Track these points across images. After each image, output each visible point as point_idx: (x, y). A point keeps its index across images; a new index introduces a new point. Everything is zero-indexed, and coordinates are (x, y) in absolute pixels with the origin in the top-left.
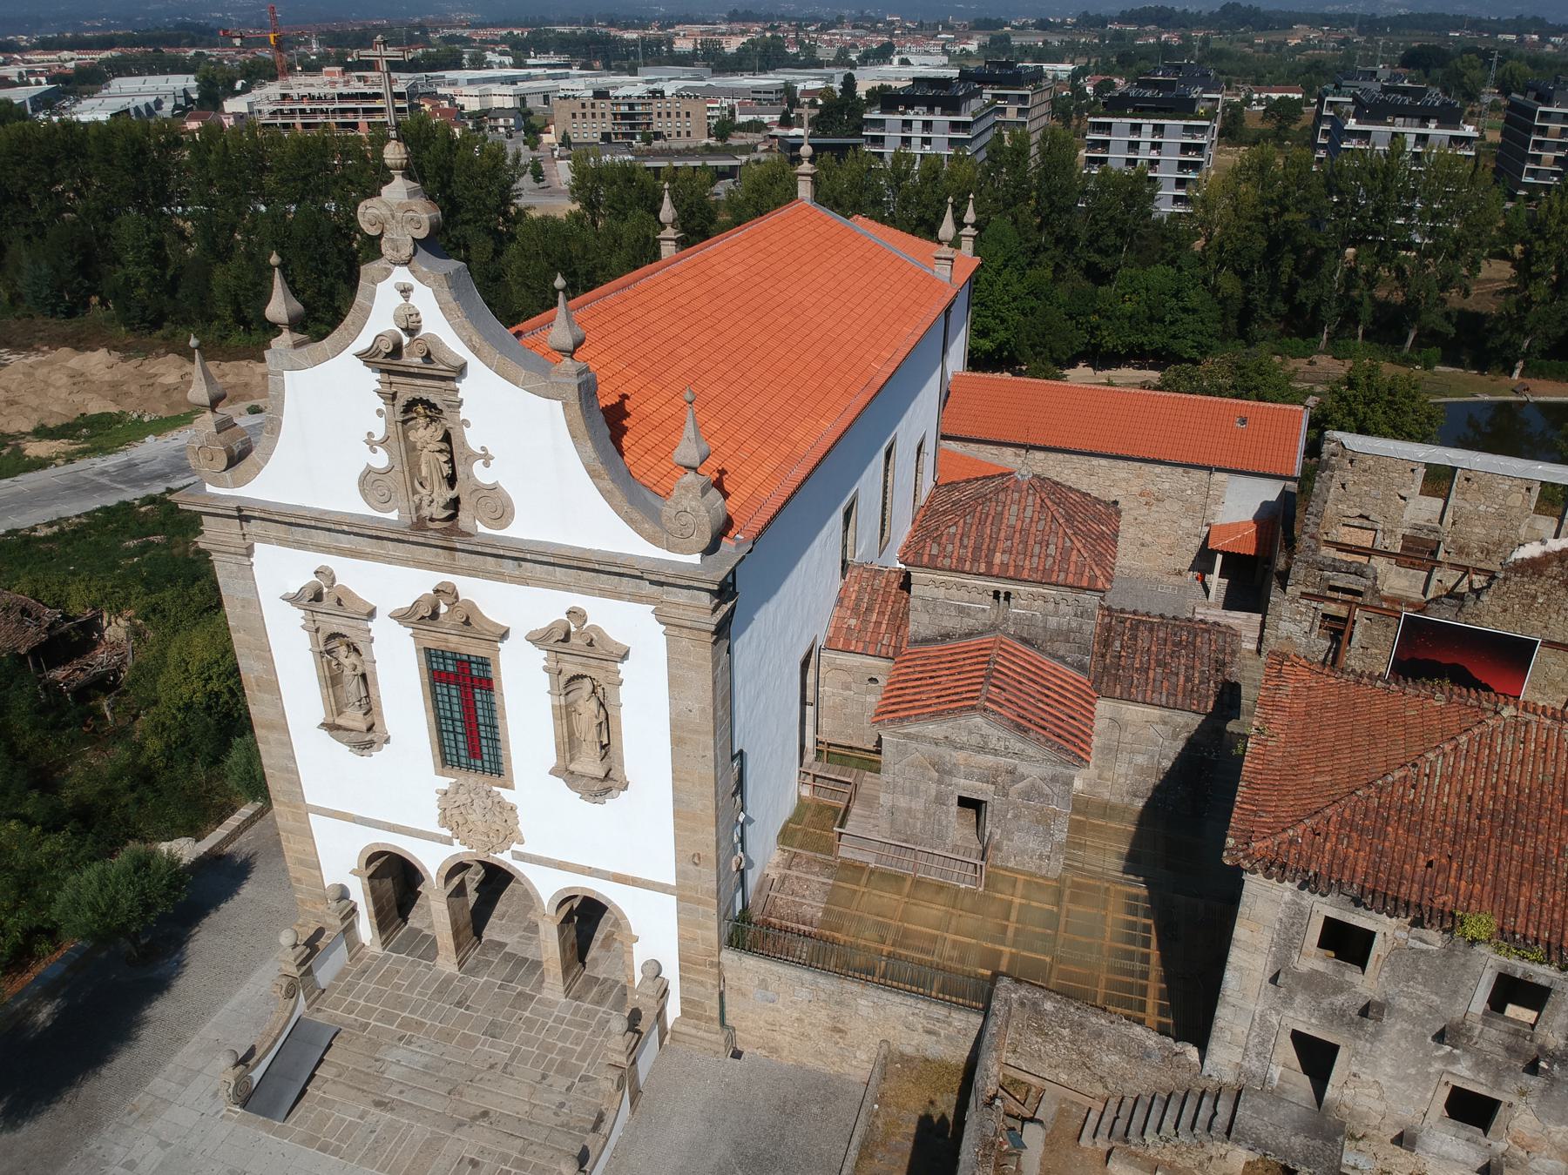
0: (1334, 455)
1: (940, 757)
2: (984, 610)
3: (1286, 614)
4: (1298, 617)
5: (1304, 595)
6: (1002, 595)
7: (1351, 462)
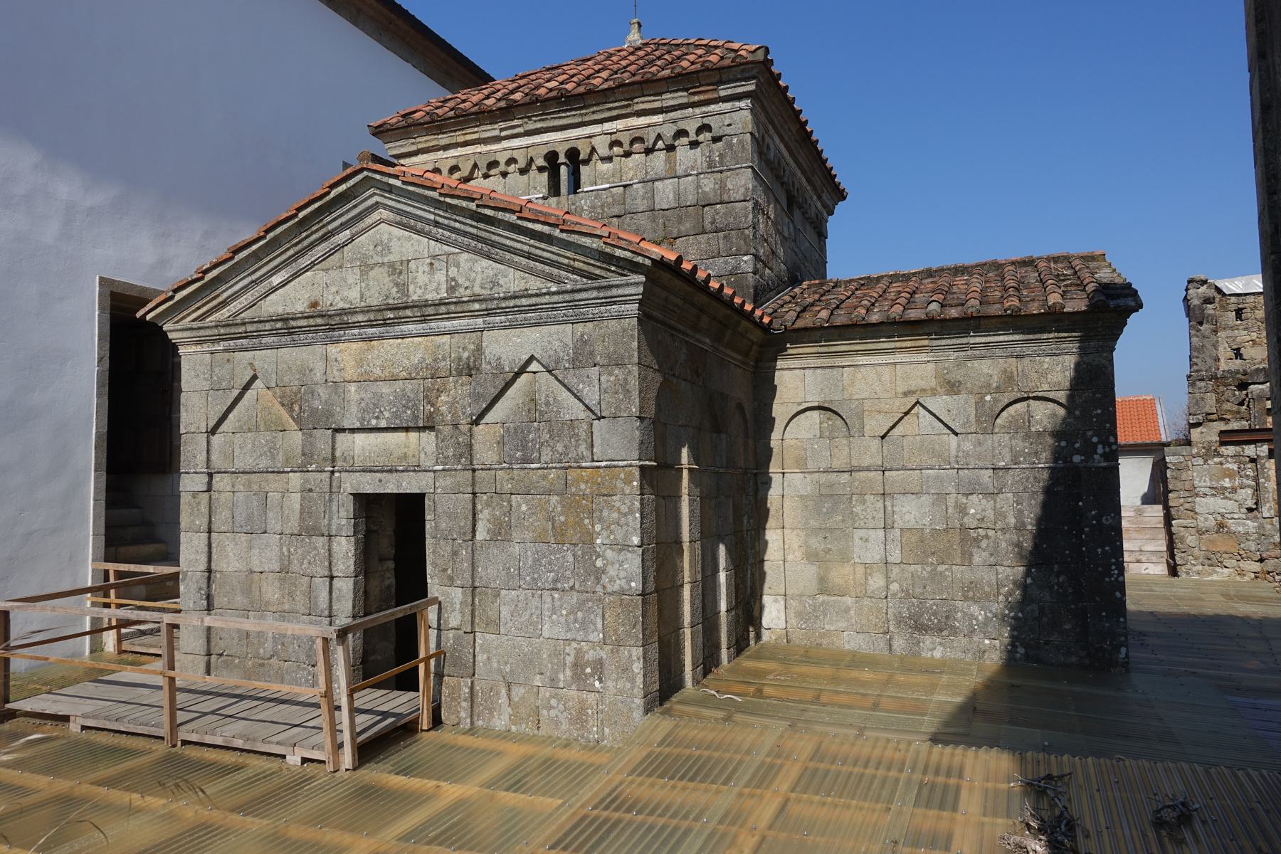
0: (1208, 301)
1: (306, 371)
3: (1202, 483)
4: (1227, 483)
5: (1228, 438)
6: (562, 159)
7: (1239, 313)
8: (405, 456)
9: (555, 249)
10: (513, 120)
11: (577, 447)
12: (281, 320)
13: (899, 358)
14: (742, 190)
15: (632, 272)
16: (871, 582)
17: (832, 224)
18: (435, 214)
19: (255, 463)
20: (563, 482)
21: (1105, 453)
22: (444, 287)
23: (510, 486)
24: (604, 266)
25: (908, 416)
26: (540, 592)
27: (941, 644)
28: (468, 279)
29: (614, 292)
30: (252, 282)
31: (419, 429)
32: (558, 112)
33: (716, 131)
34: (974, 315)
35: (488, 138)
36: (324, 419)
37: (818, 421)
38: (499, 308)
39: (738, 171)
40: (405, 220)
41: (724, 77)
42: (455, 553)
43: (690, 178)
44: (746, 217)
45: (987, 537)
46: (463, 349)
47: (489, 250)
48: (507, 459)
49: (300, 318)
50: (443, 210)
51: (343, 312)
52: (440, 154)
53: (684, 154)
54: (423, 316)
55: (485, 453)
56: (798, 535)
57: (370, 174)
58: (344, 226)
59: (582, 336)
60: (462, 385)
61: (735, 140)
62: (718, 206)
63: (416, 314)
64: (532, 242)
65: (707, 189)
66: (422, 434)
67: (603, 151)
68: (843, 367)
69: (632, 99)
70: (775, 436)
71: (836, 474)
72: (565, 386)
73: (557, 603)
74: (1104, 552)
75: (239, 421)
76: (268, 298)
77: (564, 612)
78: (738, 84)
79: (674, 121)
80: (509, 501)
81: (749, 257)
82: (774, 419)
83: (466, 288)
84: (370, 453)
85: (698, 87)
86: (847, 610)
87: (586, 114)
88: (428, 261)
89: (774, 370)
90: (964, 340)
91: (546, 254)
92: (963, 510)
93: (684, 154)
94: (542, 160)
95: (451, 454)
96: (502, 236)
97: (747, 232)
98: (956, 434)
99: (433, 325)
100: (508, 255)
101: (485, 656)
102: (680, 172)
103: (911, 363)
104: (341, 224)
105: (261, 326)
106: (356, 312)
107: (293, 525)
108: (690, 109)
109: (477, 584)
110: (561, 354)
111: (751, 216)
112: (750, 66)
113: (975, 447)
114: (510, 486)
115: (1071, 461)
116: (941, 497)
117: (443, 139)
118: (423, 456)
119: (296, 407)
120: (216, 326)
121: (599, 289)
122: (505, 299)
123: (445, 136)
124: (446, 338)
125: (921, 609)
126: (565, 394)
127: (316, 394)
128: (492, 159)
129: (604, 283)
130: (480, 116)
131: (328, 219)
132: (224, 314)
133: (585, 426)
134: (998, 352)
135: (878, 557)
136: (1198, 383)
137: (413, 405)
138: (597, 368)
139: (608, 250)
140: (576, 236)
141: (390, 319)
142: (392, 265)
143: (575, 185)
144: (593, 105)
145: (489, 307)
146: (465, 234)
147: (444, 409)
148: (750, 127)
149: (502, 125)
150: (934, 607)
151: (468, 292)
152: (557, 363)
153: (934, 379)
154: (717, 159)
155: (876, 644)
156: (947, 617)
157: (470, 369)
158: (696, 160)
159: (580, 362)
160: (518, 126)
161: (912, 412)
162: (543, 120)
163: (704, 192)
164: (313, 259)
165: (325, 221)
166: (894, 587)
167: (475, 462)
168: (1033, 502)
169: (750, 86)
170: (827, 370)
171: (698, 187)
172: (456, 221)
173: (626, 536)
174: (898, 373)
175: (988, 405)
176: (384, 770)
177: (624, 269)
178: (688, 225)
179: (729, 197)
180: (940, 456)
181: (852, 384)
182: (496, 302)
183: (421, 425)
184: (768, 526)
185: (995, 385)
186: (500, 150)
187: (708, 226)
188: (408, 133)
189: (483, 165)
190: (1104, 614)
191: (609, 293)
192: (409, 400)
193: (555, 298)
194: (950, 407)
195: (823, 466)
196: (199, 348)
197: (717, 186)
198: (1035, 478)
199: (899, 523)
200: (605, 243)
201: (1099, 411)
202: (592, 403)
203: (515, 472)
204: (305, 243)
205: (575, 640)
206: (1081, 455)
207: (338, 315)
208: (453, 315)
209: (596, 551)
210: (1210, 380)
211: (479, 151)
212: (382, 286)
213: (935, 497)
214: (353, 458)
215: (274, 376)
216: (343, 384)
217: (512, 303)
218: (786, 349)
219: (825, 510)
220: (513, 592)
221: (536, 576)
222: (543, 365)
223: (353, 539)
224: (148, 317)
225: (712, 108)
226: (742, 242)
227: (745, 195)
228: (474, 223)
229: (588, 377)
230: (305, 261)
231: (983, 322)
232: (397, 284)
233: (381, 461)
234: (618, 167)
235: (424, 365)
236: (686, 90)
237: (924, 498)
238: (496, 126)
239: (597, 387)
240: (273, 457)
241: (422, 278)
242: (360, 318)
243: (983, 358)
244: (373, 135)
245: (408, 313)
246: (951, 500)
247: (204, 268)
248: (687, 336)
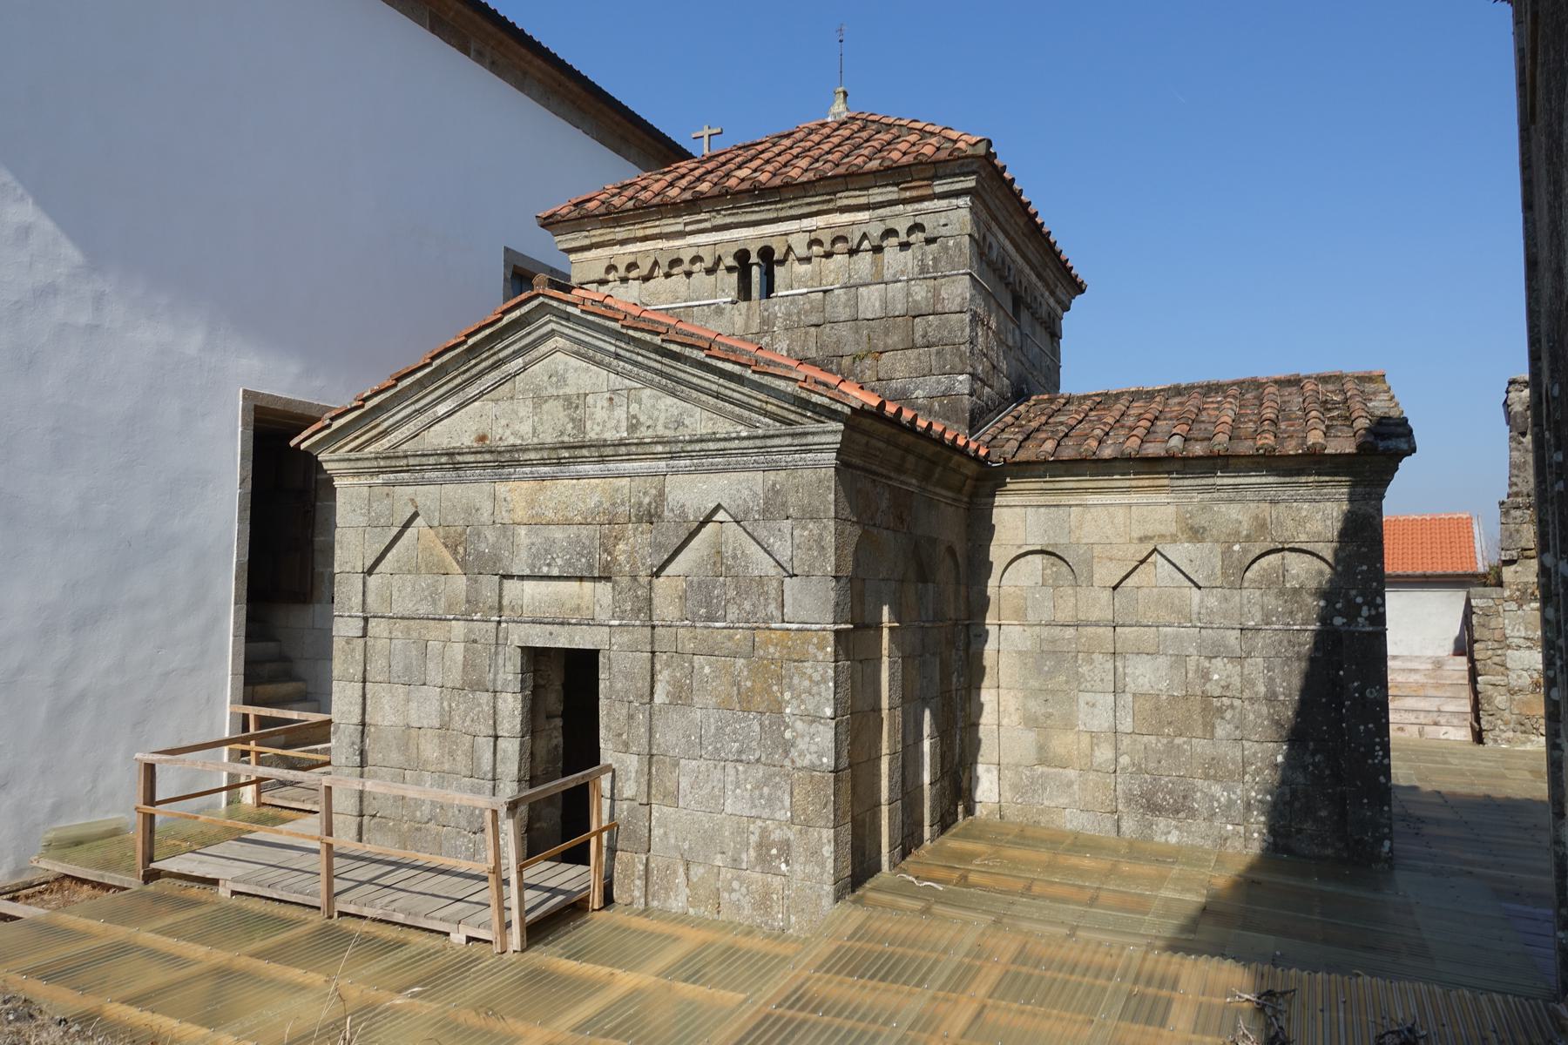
1: (471, 510)
2: (719, 311)
8: (578, 608)
9: (746, 390)
10: (699, 213)
11: (766, 606)
12: (447, 454)
13: (1134, 498)
14: (959, 300)
15: (830, 418)
16: (1097, 753)
17: (1068, 322)
18: (616, 346)
19: (414, 608)
20: (750, 644)
21: (1369, 616)
22: (624, 424)
23: (692, 645)
24: (799, 411)
25: (1144, 565)
26: (723, 763)
27: (1176, 827)
28: (650, 418)
29: (810, 439)
30: (416, 411)
31: (594, 579)
32: (751, 206)
33: (929, 233)
34: (1221, 453)
35: (672, 233)
36: (491, 564)
37: (1040, 568)
38: (684, 452)
39: (955, 278)
40: (583, 350)
41: (941, 172)
42: (631, 717)
43: (899, 284)
44: (963, 331)
45: (1232, 706)
46: (644, 493)
47: (673, 386)
48: (689, 616)
49: (466, 453)
50: (625, 343)
51: (514, 448)
52: (617, 249)
53: (893, 257)
54: (601, 456)
55: (666, 608)
56: (1015, 696)
57: (546, 300)
58: (516, 354)
59: (774, 485)
60: (642, 533)
61: (951, 243)
62: (931, 317)
63: (593, 454)
64: (721, 381)
65: (918, 298)
66: (597, 584)
67: (800, 250)
68: (1070, 506)
69: (835, 194)
70: (992, 582)
71: (1060, 628)
72: (754, 539)
73: (742, 777)
74: (1367, 730)
75: (398, 561)
76: (432, 429)
77: (749, 787)
78: (956, 179)
79: (882, 220)
80: (691, 663)
81: (965, 376)
82: (992, 563)
83: (649, 427)
84: (540, 603)
85: (911, 182)
86: (1070, 784)
87: (782, 209)
88: (607, 395)
89: (992, 506)
90: (1211, 481)
91: (736, 395)
92: (1205, 676)
93: (893, 257)
94: (732, 259)
95: (629, 608)
96: (689, 373)
97: (963, 348)
98: (1199, 588)
99: (611, 466)
100: (695, 394)
101: (662, 831)
102: (888, 277)
103: (1148, 504)
104: (514, 352)
105: (424, 460)
106: (528, 449)
107: (455, 677)
108: (901, 206)
109: (654, 752)
110: (751, 504)
111: (968, 330)
112: (970, 160)
113: (1220, 603)
114: (692, 645)
115: (1331, 624)
116: (1180, 659)
117: (621, 233)
118: (597, 608)
119: (461, 550)
120: (376, 458)
121: (793, 435)
122: (691, 442)
123: (622, 229)
124: (626, 481)
125: (1154, 787)
126: (755, 548)
127: (482, 536)
128: (675, 257)
129: (799, 429)
130: (663, 209)
131: (500, 346)
132: (385, 443)
133: (775, 584)
134: (1249, 495)
135: (1107, 725)
136: (1512, 512)
137: (589, 553)
138: (789, 521)
139: (804, 395)
140: (770, 378)
141: (565, 458)
142: (567, 398)
143: (769, 289)
144: (790, 200)
145: (674, 450)
146: (649, 368)
147: (622, 558)
148: (969, 228)
149: (687, 219)
150: (1170, 785)
151: (650, 432)
152: (746, 513)
153: (1174, 524)
154: (931, 263)
155: (1102, 824)
156: (1185, 797)
157: (651, 516)
158: (906, 264)
159: (771, 513)
160: (705, 220)
161: (1149, 560)
162: (734, 214)
163: (915, 301)
164: (482, 388)
165: (496, 349)
166: (1124, 760)
167: (654, 618)
168: (1286, 668)
169: (970, 182)
170: (1052, 509)
171: (908, 294)
172: (638, 354)
173: (818, 707)
174: (1134, 515)
175: (1236, 556)
176: (555, 953)
177: (821, 415)
178: (896, 338)
179: (943, 307)
180: (1180, 612)
181: (1080, 527)
182: (680, 445)
183: (597, 575)
184: (983, 685)
185: (1245, 533)
186: (684, 247)
187: (919, 340)
188: (580, 225)
189: (664, 262)
190: (1365, 801)
191: (804, 441)
192: (584, 547)
193: (746, 443)
194: (1193, 557)
195: (1046, 618)
196: (356, 481)
197: (930, 295)
198: (1290, 641)
199: (1131, 687)
200: (800, 387)
201: (1365, 568)
202: (784, 560)
203: (698, 631)
204: (474, 371)
205: (760, 818)
206: (1343, 617)
207: (508, 451)
208: (633, 457)
209: (784, 721)
210: (1528, 508)
211: (660, 246)
212: (556, 421)
213: (1173, 658)
214: (522, 607)
215: (437, 514)
216: (512, 527)
217: (698, 447)
218: (1005, 484)
219: (1046, 669)
220: (694, 762)
221: (719, 745)
222: (731, 515)
223: (519, 696)
224: (303, 446)
225: (926, 205)
226: (957, 359)
227: (962, 306)
228: (659, 358)
229: (779, 530)
230: (472, 391)
231: (1231, 461)
232: (573, 420)
233: (553, 612)
234: (817, 269)
235: (601, 509)
236: (897, 185)
237: (1161, 659)
238: (680, 220)
239: (789, 542)
240: (434, 603)
241: (600, 414)
242: (532, 455)
243: (1231, 501)
244: (542, 226)
245: (585, 452)
246: (1192, 663)
247: (365, 395)
248: (891, 479)
